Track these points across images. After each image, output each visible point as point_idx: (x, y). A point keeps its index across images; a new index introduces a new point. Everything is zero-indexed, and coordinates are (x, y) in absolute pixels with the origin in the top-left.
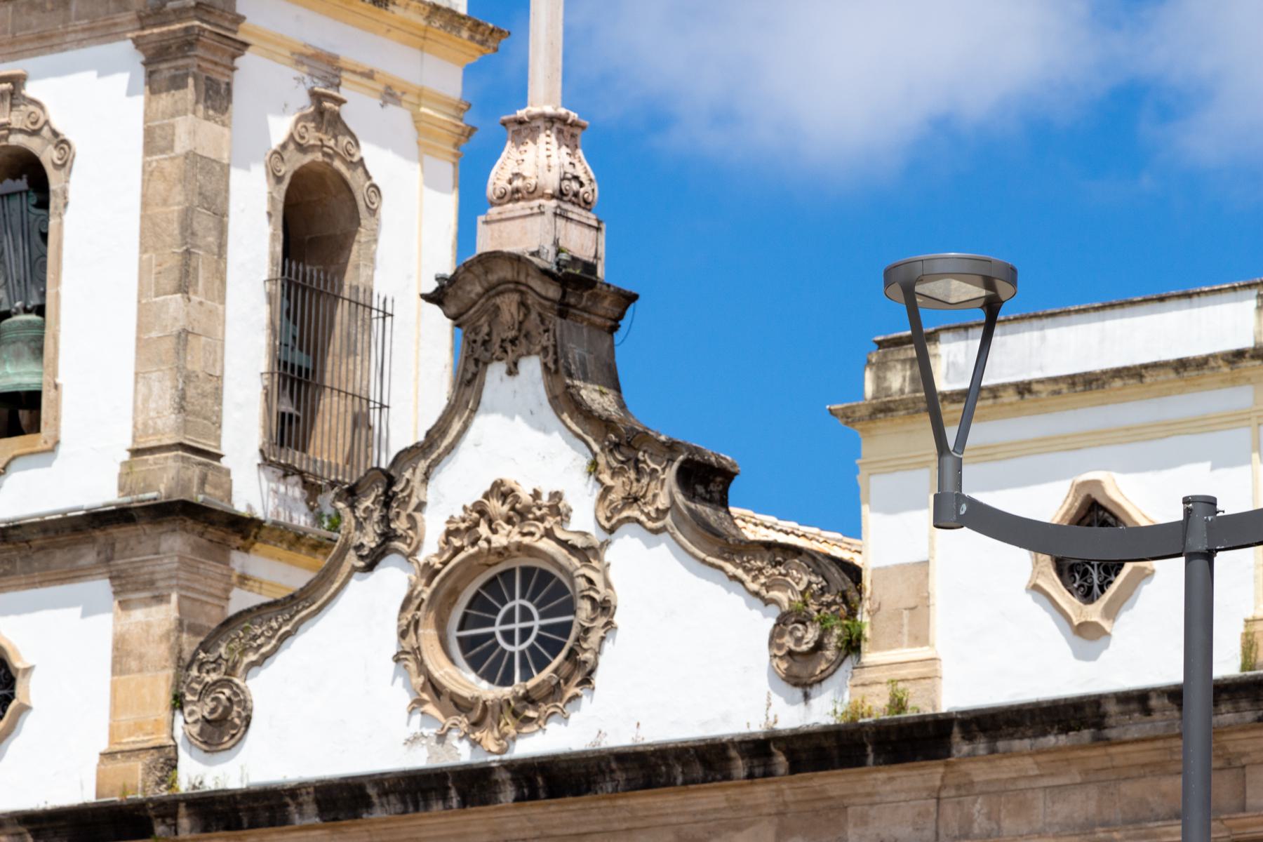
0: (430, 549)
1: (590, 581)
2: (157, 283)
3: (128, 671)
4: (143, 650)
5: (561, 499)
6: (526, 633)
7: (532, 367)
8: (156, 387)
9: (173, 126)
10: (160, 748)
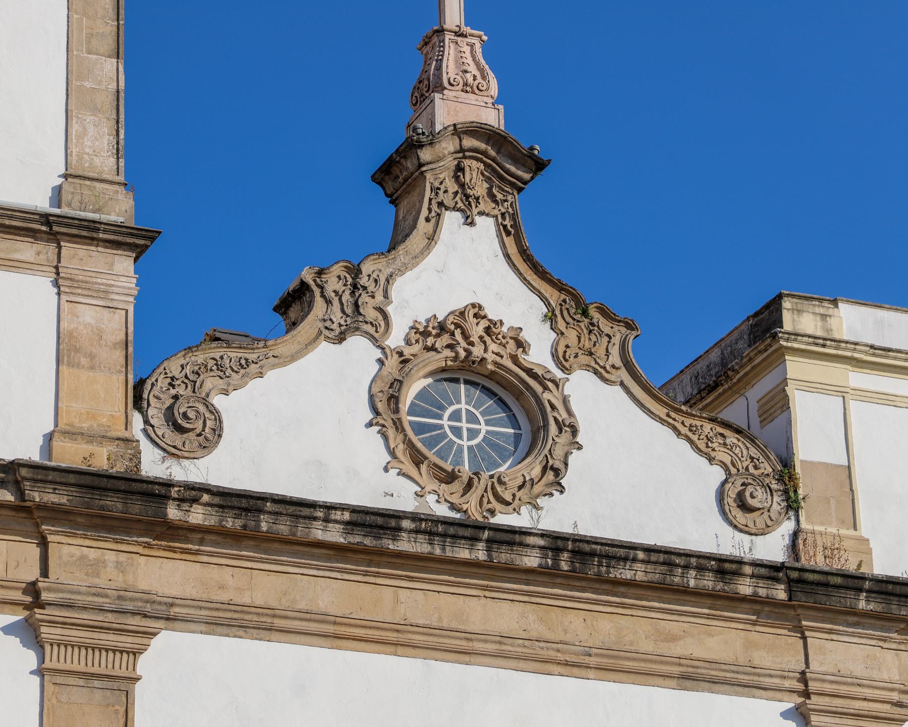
0: (395, 339)
2: (89, 43)
3: (78, 365)
4: (94, 351)
6: (457, 431)
7: (486, 226)
8: (91, 130)
10: (126, 440)
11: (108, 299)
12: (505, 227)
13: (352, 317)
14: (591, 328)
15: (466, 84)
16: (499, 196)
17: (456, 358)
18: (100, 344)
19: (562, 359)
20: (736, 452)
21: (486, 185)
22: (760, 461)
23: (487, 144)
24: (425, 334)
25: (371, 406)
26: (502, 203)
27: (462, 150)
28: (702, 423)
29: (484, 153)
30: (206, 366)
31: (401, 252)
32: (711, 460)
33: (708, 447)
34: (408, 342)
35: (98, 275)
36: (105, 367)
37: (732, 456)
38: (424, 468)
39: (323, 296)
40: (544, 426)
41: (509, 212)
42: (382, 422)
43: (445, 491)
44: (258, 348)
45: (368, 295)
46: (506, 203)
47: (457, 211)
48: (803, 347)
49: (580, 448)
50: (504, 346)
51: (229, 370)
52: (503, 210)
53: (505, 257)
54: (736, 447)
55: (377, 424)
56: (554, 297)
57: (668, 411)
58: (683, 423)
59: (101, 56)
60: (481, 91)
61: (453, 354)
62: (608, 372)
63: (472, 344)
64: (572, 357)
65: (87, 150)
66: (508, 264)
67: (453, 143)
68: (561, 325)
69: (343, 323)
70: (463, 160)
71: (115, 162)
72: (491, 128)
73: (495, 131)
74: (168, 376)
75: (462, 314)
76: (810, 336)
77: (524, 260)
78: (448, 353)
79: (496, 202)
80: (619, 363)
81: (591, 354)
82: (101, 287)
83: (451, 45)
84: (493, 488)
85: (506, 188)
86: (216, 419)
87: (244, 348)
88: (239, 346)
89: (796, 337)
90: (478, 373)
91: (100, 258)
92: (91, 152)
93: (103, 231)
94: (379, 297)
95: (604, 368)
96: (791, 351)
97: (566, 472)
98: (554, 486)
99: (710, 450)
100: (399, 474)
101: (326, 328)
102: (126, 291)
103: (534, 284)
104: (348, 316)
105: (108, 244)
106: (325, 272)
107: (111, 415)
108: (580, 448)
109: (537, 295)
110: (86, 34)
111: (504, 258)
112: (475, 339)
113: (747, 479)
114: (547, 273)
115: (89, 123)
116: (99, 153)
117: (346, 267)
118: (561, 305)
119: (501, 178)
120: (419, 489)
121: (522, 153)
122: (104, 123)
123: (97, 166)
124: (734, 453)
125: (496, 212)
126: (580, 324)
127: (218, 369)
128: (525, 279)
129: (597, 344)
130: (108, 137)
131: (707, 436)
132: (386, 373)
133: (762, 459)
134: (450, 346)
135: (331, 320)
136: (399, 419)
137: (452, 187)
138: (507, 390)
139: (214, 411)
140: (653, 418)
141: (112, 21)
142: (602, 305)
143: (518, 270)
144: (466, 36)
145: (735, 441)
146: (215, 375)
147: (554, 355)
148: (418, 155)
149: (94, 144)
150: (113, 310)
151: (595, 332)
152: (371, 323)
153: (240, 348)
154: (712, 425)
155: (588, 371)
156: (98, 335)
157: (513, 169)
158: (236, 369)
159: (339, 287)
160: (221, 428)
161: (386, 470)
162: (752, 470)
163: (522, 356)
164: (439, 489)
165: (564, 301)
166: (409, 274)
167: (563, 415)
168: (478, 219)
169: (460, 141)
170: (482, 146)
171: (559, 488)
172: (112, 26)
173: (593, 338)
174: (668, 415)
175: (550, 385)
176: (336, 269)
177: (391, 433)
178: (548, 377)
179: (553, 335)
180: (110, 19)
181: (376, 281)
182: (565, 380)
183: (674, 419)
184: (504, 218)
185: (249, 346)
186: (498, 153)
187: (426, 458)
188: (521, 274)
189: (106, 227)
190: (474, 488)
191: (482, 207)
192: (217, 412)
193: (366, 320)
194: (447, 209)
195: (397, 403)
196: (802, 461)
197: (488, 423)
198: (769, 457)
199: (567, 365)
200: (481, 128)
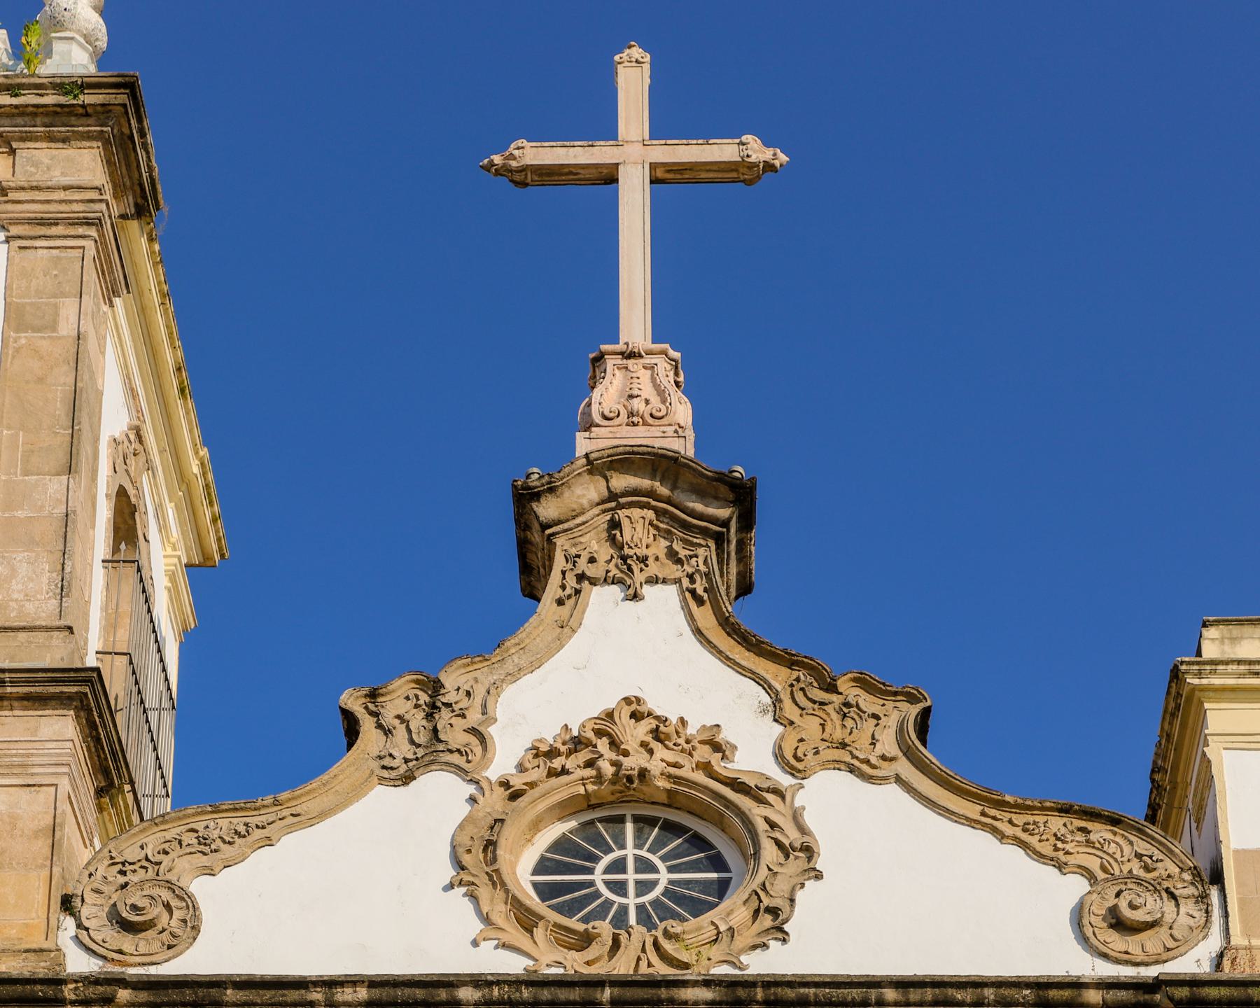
1: (773, 825)
5: (719, 732)
8: (23, 570)
9: (56, 306)
11: (27, 774)
12: (693, 592)
13: (426, 747)
14: (846, 710)
15: (631, 414)
16: (683, 553)
17: (599, 778)
18: (12, 835)
19: (793, 762)
20: (1110, 851)
21: (664, 543)
22: (1154, 858)
23: (653, 478)
24: (552, 753)
25: (457, 866)
26: (688, 560)
27: (613, 496)
28: (1045, 818)
29: (651, 494)
30: (180, 843)
31: (513, 651)
32: (1061, 867)
33: (1056, 849)
34: (521, 768)
35: (12, 746)
36: (18, 864)
37: (1102, 858)
38: (539, 932)
39: (380, 726)
40: (755, 854)
41: (697, 571)
42: (471, 879)
43: (575, 961)
44: (264, 806)
45: (454, 714)
46: (695, 559)
47: (613, 583)
48: (1231, 682)
49: (819, 876)
50: (690, 754)
51: (219, 842)
52: (690, 570)
53: (695, 635)
54: (1109, 843)
55: (460, 884)
56: (779, 676)
57: (982, 807)
58: (1010, 822)
59: (44, 475)
60: (662, 418)
61: (594, 773)
62: (874, 767)
63: (626, 754)
64: (810, 756)
65: (15, 596)
66: (701, 642)
67: (595, 488)
68: (790, 710)
69: (410, 756)
70: (618, 511)
71: (58, 605)
72: (649, 449)
73: (657, 453)
74: (117, 860)
75: (610, 715)
76: (1239, 662)
77: (729, 634)
78: (590, 772)
79: (679, 561)
80: (891, 748)
81: (843, 745)
82: (15, 759)
83: (617, 371)
84: (656, 944)
85: (695, 540)
86: (188, 907)
87: (242, 809)
88: (231, 807)
89: (1214, 667)
90: (653, 803)
91: (18, 724)
92: (21, 597)
93: (11, 682)
94: (474, 717)
95: (867, 762)
96: (1211, 694)
97: (792, 911)
98: (772, 933)
99: (1061, 853)
100: (496, 947)
101: (384, 767)
102: (54, 760)
103: (743, 663)
104: (418, 746)
105: (26, 703)
106: (380, 691)
107: (24, 924)
108: (819, 876)
109: (749, 678)
110: (22, 451)
111: (693, 636)
112: (631, 744)
113: (1126, 883)
114: (763, 643)
115: (20, 561)
116: (34, 596)
117: (417, 682)
118: (792, 685)
119: (685, 526)
120: (496, 942)
121: (707, 477)
122: (43, 557)
123: (29, 614)
124: (1105, 852)
125: (679, 574)
126: (825, 707)
127: (200, 843)
128: (728, 658)
129: (854, 730)
130: (49, 574)
131: (1055, 835)
132: (481, 814)
133: (1158, 855)
134: (590, 764)
135: (391, 755)
136: (497, 871)
137: (604, 552)
138: (705, 820)
139: (185, 896)
140: (956, 821)
141: (65, 430)
142: (861, 673)
143: (715, 647)
144: (640, 356)
145: (1109, 836)
146: (193, 850)
147: (779, 755)
148: (535, 512)
149: (27, 587)
150: (37, 788)
151: (852, 714)
152: (459, 751)
153: (236, 809)
154: (1065, 820)
155: (839, 769)
156: (10, 823)
157: (699, 507)
158: (227, 839)
159: (403, 707)
160: (196, 915)
161: (475, 943)
162: (1142, 873)
163: (723, 764)
164: (565, 958)
165: (798, 680)
166: (527, 680)
167: (791, 835)
168: (647, 590)
169: (607, 481)
170: (645, 483)
171: (780, 936)
172: (63, 434)
173: (849, 723)
174: (983, 814)
175: (770, 797)
176: (400, 687)
177: (484, 892)
178: (765, 786)
179: (779, 729)
180: (62, 427)
181: (468, 694)
182: (797, 786)
183: (994, 818)
184: (692, 580)
185: (248, 805)
186: (674, 488)
187: (541, 918)
188: (720, 652)
189: (13, 675)
190: (622, 949)
191: (653, 569)
192: (189, 897)
193: (450, 747)
194: (593, 582)
195: (495, 850)
196: (1236, 852)
197: (671, 869)
198: (1171, 851)
199: (799, 766)
200: (633, 453)
